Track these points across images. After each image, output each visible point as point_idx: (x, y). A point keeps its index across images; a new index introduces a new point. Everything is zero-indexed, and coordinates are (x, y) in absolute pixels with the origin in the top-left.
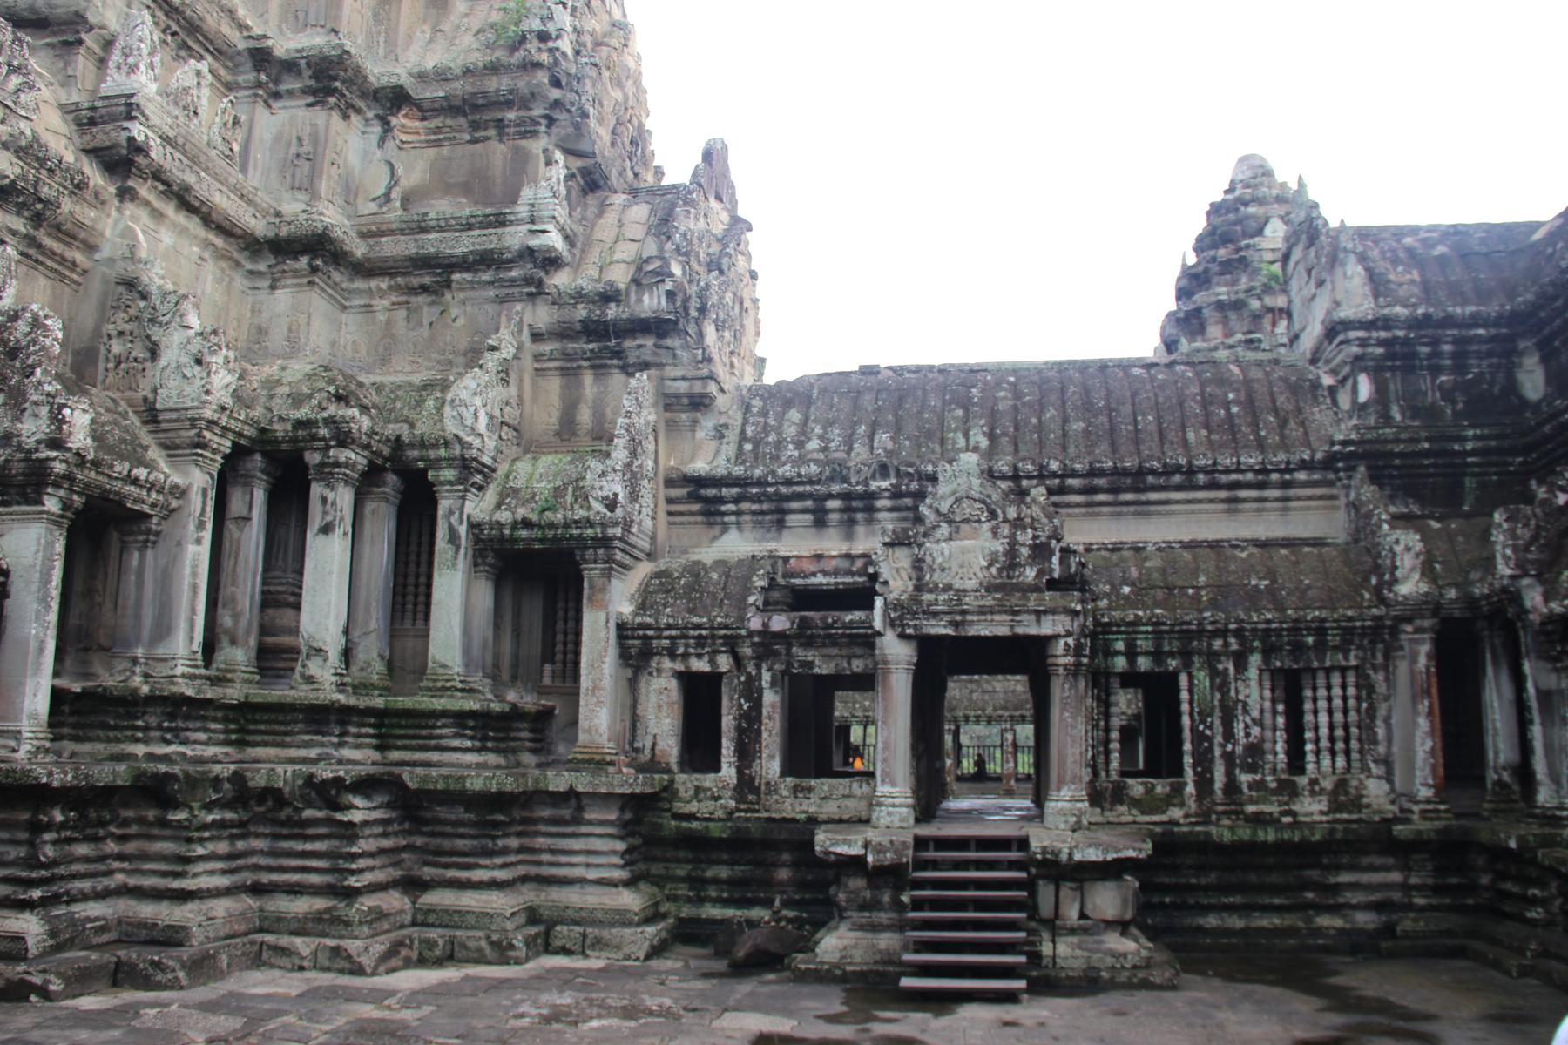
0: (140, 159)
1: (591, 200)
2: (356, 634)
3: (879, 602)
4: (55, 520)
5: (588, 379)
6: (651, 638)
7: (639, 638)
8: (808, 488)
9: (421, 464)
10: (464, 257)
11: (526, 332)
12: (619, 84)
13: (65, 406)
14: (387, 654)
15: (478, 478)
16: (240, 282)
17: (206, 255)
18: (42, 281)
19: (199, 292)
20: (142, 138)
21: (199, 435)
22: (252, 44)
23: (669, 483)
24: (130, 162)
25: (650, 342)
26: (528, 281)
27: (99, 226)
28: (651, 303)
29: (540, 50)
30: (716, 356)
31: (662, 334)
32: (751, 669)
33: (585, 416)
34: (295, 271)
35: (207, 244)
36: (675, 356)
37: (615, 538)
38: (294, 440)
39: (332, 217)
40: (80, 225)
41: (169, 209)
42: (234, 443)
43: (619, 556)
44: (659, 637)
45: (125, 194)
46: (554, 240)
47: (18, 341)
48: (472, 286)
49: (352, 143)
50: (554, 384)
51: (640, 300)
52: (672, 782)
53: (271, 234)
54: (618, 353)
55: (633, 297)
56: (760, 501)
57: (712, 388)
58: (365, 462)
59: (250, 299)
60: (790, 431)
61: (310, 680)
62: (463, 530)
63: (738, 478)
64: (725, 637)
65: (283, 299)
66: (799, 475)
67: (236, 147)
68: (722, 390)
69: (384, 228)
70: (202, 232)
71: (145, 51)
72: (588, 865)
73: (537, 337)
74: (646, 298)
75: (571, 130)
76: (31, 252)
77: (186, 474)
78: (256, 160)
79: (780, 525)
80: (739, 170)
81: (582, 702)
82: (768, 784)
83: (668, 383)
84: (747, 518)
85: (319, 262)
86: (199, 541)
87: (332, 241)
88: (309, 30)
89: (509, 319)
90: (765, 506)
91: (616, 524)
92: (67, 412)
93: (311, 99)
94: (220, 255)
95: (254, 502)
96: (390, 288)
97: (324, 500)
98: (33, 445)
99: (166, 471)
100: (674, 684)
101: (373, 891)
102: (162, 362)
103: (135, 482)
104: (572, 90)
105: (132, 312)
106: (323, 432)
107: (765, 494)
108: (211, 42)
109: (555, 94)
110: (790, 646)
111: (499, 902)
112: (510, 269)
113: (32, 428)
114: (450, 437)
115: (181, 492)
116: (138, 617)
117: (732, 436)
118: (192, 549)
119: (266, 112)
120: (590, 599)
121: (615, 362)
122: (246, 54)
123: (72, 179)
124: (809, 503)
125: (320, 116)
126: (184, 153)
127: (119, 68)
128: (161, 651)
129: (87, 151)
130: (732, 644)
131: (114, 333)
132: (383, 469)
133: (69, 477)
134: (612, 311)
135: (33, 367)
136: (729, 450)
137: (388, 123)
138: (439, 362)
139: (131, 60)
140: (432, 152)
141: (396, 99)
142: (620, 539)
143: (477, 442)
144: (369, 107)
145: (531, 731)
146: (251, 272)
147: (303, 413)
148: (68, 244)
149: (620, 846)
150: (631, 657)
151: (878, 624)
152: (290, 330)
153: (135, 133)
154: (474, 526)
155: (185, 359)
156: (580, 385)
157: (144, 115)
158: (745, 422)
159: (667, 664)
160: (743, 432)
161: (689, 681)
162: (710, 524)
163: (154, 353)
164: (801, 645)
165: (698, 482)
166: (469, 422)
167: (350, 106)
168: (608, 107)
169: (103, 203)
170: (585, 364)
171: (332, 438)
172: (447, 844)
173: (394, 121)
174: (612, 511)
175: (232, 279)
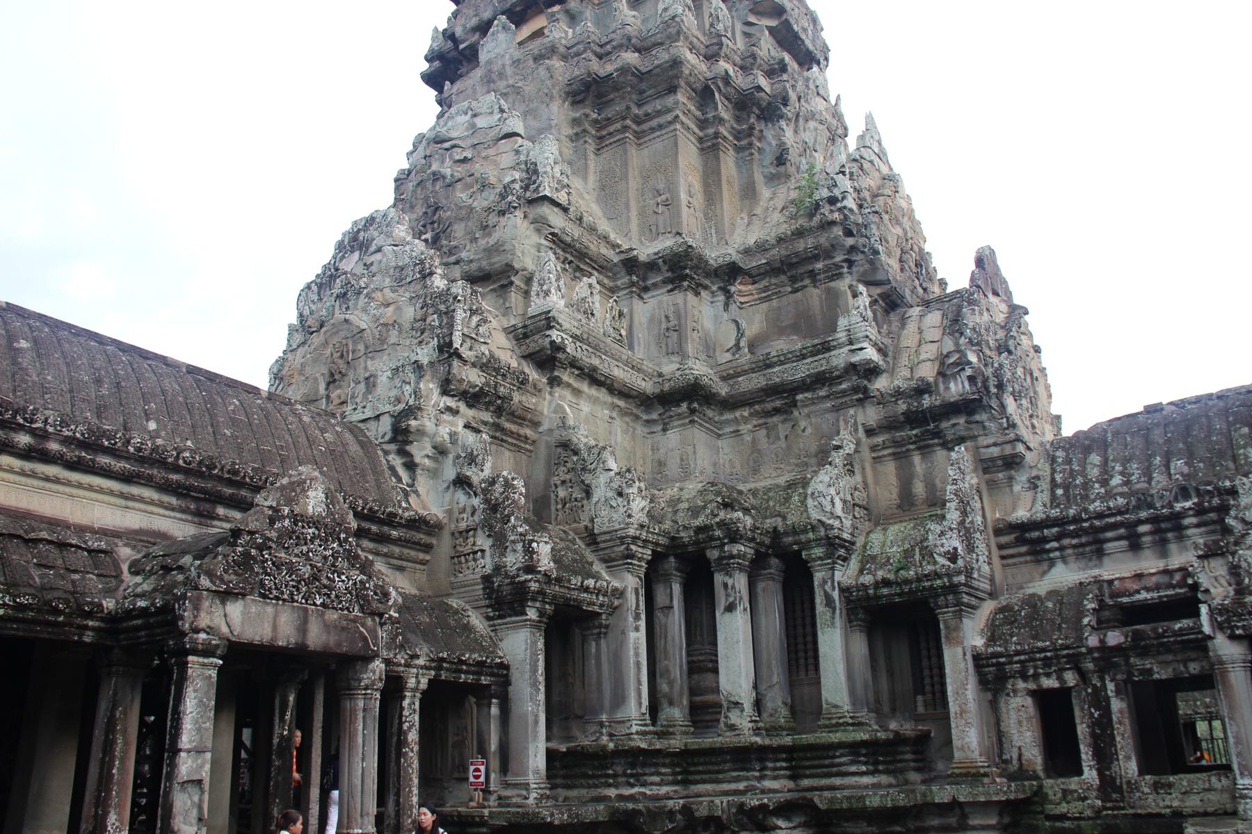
0: (560, 355)
1: (894, 317)
2: (763, 687)
3: (1204, 609)
4: (535, 625)
5: (917, 459)
6: (1004, 664)
7: (993, 665)
8: (1119, 518)
9: (796, 547)
10: (803, 380)
11: (861, 430)
12: (898, 223)
13: (533, 541)
14: (789, 701)
15: (842, 552)
16: (640, 430)
17: (614, 415)
18: (507, 453)
21: (627, 549)
22: (623, 256)
23: (998, 532)
24: (554, 359)
25: (961, 420)
26: (856, 390)
27: (539, 408)
28: (957, 388)
29: (832, 211)
30: (1018, 422)
33: (919, 489)
34: (679, 415)
35: (614, 407)
36: (984, 428)
37: (960, 584)
38: (697, 543)
39: (699, 369)
40: (527, 409)
41: (584, 386)
42: (653, 551)
43: (966, 599)
44: (1011, 663)
45: (554, 382)
46: (871, 354)
48: (813, 402)
49: (705, 312)
50: (890, 468)
51: (947, 388)
52: (1041, 787)
53: (657, 391)
54: (938, 434)
55: (941, 387)
56: (1078, 536)
57: (1020, 448)
58: (752, 551)
59: (649, 441)
60: (1094, 473)
61: (732, 727)
62: (836, 595)
63: (1056, 519)
64: (1067, 656)
65: (673, 437)
66: (1109, 508)
67: (623, 333)
68: (1029, 448)
71: (553, 280)
73: (870, 432)
74: (952, 385)
75: (867, 266)
76: (498, 434)
77: (622, 579)
79: (1100, 554)
80: (1008, 267)
81: (953, 725)
82: (1129, 782)
83: (982, 450)
84: (1070, 551)
85: (696, 405)
86: (637, 629)
87: (702, 387)
88: (661, 238)
89: (846, 422)
90: (1083, 540)
91: (959, 573)
92: (534, 545)
93: (670, 287)
94: (624, 413)
95: (674, 593)
96: (751, 414)
97: (725, 585)
98: (515, 572)
99: (608, 580)
100: (1029, 701)
102: (595, 499)
103: (587, 590)
104: (862, 236)
105: (569, 465)
106: (718, 533)
107: (1082, 529)
108: (596, 262)
109: (850, 241)
110: (1127, 658)
112: (840, 383)
113: (514, 560)
114: (815, 522)
115: (620, 593)
116: (600, 691)
117: (1044, 485)
118: (632, 635)
119: (640, 303)
120: (947, 637)
121: (936, 441)
124: (1122, 531)
125: (678, 297)
128: (619, 716)
129: (524, 357)
130: (1075, 662)
131: (558, 483)
132: (767, 555)
133: (541, 592)
134: (927, 401)
135: (509, 516)
136: (1044, 497)
137: (729, 291)
138: (797, 465)
139: (545, 288)
140: (765, 306)
141: (731, 272)
142: (965, 585)
143: (836, 523)
144: (713, 283)
145: (914, 753)
146: (648, 421)
147: (699, 521)
148: (520, 425)
150: (988, 682)
151: (1207, 629)
152: (682, 460)
153: (554, 338)
154: (844, 590)
155: (610, 494)
156: (911, 464)
158: (1053, 471)
159: (1021, 685)
160: (1053, 480)
161: (1040, 696)
162: (1038, 562)
163: (588, 493)
164: (1138, 655)
165: (1021, 529)
166: (828, 509)
167: (699, 285)
168: (893, 242)
169: (540, 391)
170: (912, 447)
173: (733, 289)
174: (954, 563)
175: (634, 429)
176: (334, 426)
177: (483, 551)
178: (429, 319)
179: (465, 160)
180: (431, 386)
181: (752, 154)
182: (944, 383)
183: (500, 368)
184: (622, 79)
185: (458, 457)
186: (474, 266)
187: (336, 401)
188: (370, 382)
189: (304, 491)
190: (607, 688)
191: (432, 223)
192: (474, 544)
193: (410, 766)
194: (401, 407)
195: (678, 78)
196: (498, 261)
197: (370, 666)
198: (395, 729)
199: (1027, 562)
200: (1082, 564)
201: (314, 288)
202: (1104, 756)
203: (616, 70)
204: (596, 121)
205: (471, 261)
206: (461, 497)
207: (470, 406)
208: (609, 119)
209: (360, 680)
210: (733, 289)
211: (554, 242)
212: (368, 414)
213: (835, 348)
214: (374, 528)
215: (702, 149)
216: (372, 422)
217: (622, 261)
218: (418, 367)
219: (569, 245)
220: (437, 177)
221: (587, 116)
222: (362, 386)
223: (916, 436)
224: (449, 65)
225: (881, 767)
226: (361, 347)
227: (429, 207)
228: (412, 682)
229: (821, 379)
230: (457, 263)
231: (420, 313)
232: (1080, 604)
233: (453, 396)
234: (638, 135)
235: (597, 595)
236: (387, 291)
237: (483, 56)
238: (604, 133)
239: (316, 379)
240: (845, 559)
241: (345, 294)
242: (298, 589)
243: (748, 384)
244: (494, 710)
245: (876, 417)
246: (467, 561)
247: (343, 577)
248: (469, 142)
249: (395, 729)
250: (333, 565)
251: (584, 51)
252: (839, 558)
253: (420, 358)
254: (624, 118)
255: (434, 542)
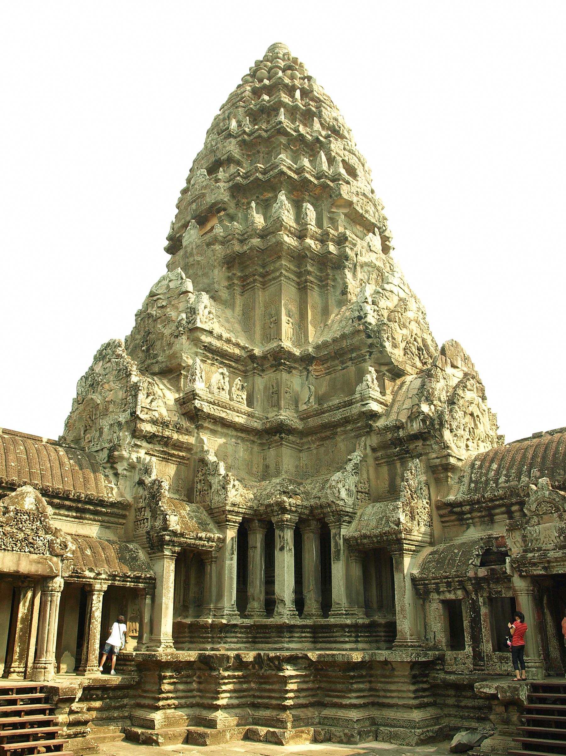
3: (508, 560)
6: (427, 584)
8: (501, 502)
12: (405, 326)
15: (347, 518)
16: (256, 449)
17: (239, 441)
19: (237, 457)
20: (199, 405)
22: (248, 354)
24: (197, 415)
25: (420, 443)
28: (416, 426)
29: (360, 325)
31: (425, 440)
32: (474, 597)
35: (237, 438)
38: (266, 513)
43: (406, 547)
44: (431, 584)
45: (199, 427)
47: (155, 492)
48: (345, 432)
49: (294, 381)
50: (385, 470)
51: (412, 426)
52: (444, 655)
56: (481, 511)
58: (297, 518)
59: (262, 454)
61: (280, 614)
65: (272, 452)
69: (309, 415)
70: (234, 433)
72: (399, 698)
75: (379, 355)
78: (257, 398)
79: (492, 521)
83: (431, 461)
84: (477, 520)
85: (283, 435)
90: (483, 514)
95: (257, 540)
97: (280, 536)
101: (299, 708)
102: (213, 490)
103: (201, 539)
107: (482, 507)
108: (233, 358)
109: (370, 341)
111: (354, 715)
112: (358, 423)
114: (330, 502)
116: (210, 592)
117: (466, 480)
118: (228, 562)
119: (260, 378)
120: (396, 568)
122: (248, 358)
123: (176, 427)
124: (503, 509)
125: (278, 375)
126: (219, 406)
127: (190, 381)
128: (219, 605)
129: (183, 415)
130: (462, 585)
134: (401, 433)
135: (158, 501)
136: (464, 488)
137: (308, 370)
139: (194, 377)
140: (328, 377)
141: (307, 360)
143: (341, 503)
144: (300, 365)
145: (385, 632)
147: (266, 502)
149: (412, 688)
151: (508, 571)
154: (346, 540)
155: (219, 488)
156: (395, 468)
157: (199, 397)
158: (472, 473)
159: (436, 596)
160: (471, 478)
161: (446, 603)
164: (494, 583)
165: (452, 505)
167: (291, 367)
168: (399, 338)
169: (190, 432)
170: (396, 458)
171: (279, 510)
172: (333, 687)
173: (311, 368)
174: (398, 527)
175: (252, 448)
176: (78, 455)
177: (147, 519)
178: (128, 398)
179: (163, 307)
180: (126, 433)
181: (328, 290)
182: (410, 422)
183: (164, 422)
184: (252, 254)
185: (141, 469)
186: (164, 365)
187: (87, 441)
188: (101, 431)
189: (23, 498)
190: (214, 590)
191: (147, 341)
192: (144, 515)
193: (94, 629)
194: (111, 444)
195: (281, 251)
196: (174, 362)
197: (54, 580)
198: (89, 610)
199: (455, 525)
200: (483, 527)
201: (84, 379)
202: (476, 640)
203: (248, 249)
204: (241, 277)
205: (163, 362)
206: (141, 491)
207: (149, 443)
208: (247, 276)
209: (49, 587)
210: (311, 368)
211: (206, 350)
212: (99, 448)
213: (355, 403)
214: (91, 508)
215: (299, 289)
216: (100, 452)
217: (248, 356)
218: (119, 424)
219: (215, 351)
220: (150, 316)
221: (234, 274)
222: (98, 434)
223: (397, 452)
224: (174, 245)
225: (359, 639)
226: (98, 413)
227: (145, 332)
228: (97, 587)
229: (346, 421)
230: (157, 363)
231: (125, 395)
232: (470, 552)
233: (138, 438)
234: (264, 284)
235: (208, 542)
236: (111, 383)
237: (184, 243)
238: (245, 283)
239: (80, 428)
240: (350, 522)
241: (93, 384)
242: (16, 545)
243: (313, 422)
244: (148, 601)
245: (376, 441)
246: (141, 524)
247: (41, 538)
248: (167, 296)
249: (89, 610)
250: (36, 533)
251: (232, 239)
252: (344, 521)
253: (120, 419)
254: (254, 275)
255: (127, 514)
